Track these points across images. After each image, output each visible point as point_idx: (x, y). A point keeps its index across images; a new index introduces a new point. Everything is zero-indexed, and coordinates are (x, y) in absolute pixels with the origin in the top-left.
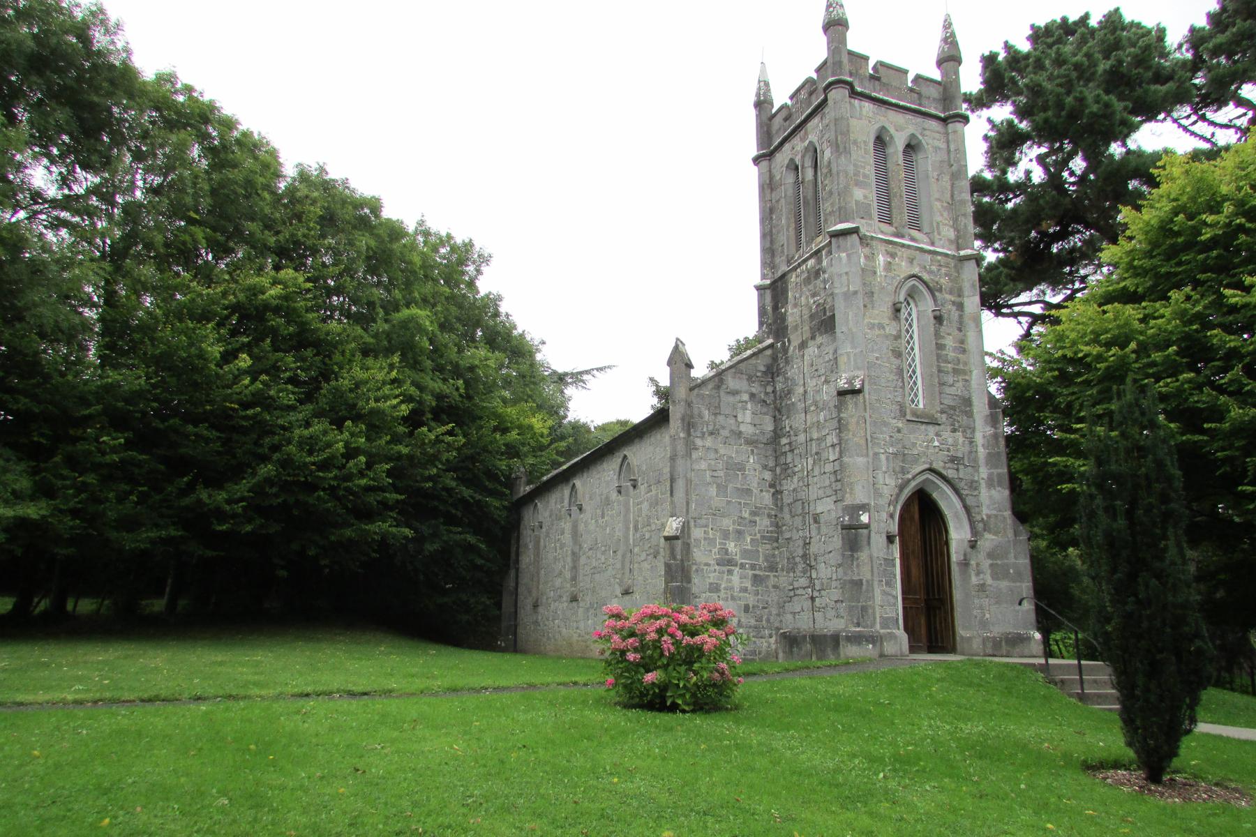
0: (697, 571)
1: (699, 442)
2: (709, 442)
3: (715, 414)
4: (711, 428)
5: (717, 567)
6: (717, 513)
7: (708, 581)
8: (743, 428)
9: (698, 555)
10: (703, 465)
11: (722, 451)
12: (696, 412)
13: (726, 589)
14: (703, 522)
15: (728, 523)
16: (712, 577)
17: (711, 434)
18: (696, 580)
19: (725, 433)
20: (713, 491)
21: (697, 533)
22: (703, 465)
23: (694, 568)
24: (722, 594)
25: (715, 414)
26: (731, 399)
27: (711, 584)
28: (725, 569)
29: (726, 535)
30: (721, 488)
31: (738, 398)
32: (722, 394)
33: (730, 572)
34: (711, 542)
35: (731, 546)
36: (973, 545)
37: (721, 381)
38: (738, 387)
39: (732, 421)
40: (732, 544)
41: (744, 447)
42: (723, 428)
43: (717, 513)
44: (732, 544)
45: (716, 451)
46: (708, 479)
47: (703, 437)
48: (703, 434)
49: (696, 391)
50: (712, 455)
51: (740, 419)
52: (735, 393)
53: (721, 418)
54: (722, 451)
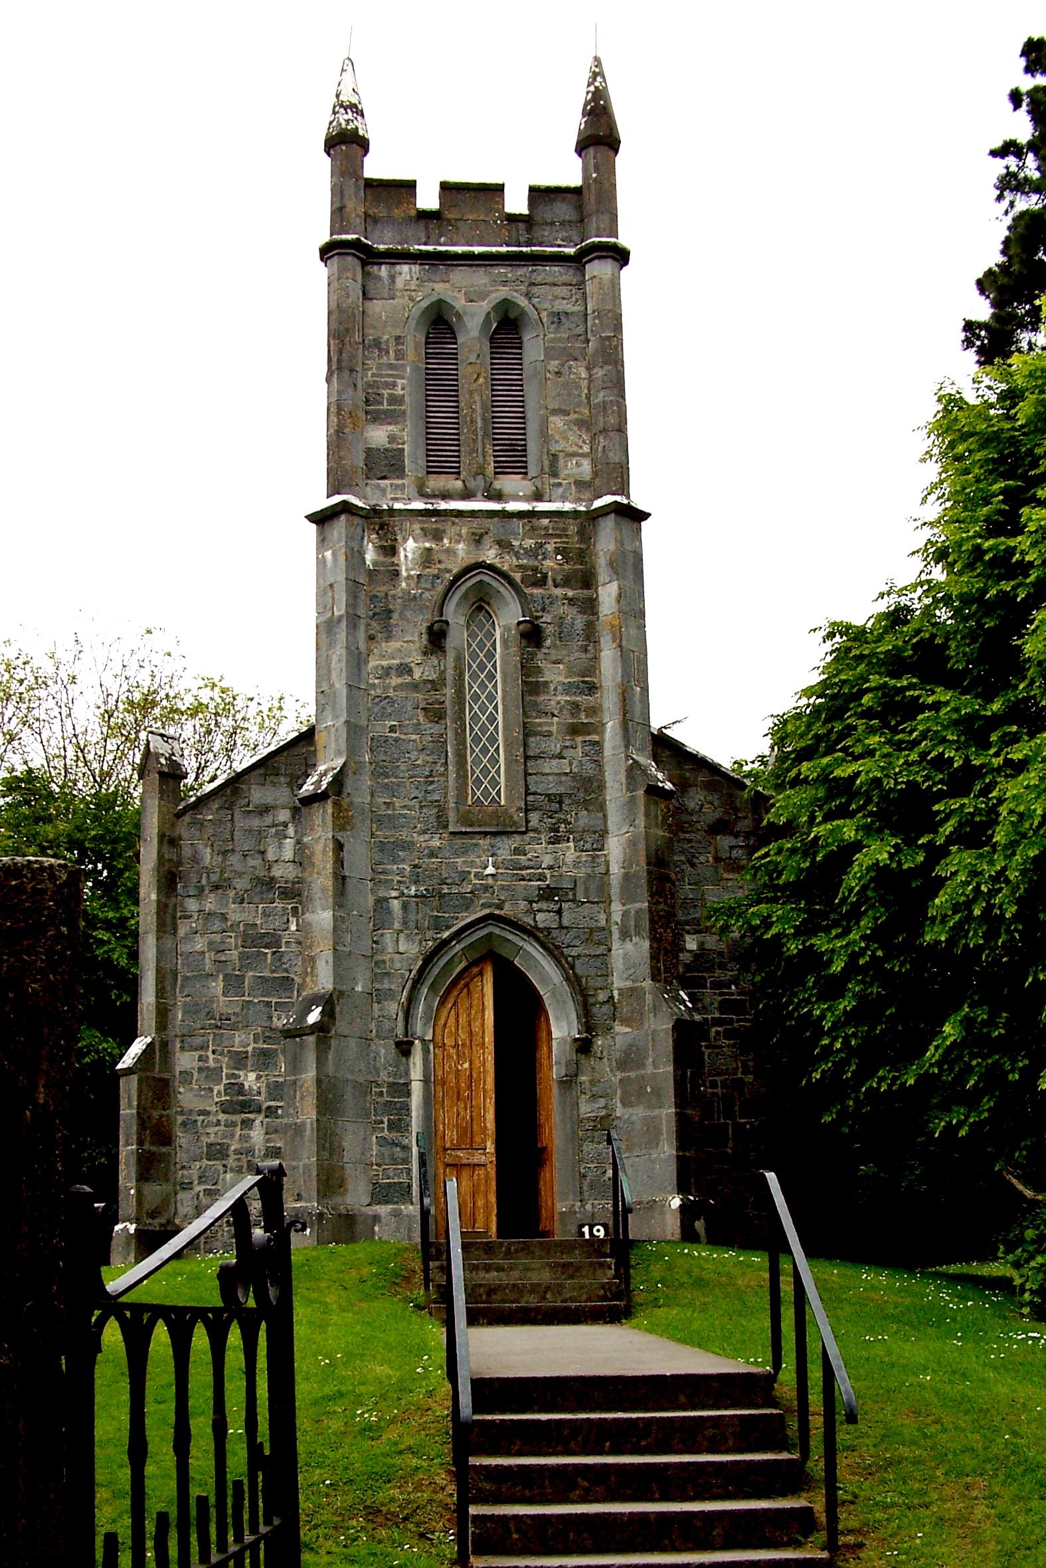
0: (184, 1124)
1: (192, 905)
2: (211, 903)
3: (224, 853)
4: (215, 878)
5: (222, 1117)
6: (224, 1023)
7: (205, 1140)
8: (277, 872)
9: (187, 1097)
10: (200, 944)
11: (234, 917)
12: (187, 852)
13: (237, 1152)
14: (198, 1041)
15: (243, 1041)
16: (213, 1135)
18: (182, 1138)
19: (241, 884)
20: (217, 986)
21: (185, 1061)
22: (200, 944)
23: (180, 1119)
24: (231, 1161)
25: (224, 853)
26: (255, 822)
27: (210, 1145)
28: (237, 1118)
29: (240, 1060)
30: (234, 983)
31: (268, 820)
32: (238, 815)
33: (247, 1124)
34: (213, 1074)
35: (250, 1079)
36: (584, 1046)
38: (269, 800)
39: (255, 862)
40: (252, 1076)
41: (279, 905)
42: (240, 875)
43: (224, 1023)
44: (252, 1076)
45: (224, 918)
46: (208, 966)
47: (200, 894)
48: (201, 890)
49: (187, 819)
50: (217, 925)
51: (271, 856)
52: (265, 810)
53: (234, 860)
54: (234, 917)
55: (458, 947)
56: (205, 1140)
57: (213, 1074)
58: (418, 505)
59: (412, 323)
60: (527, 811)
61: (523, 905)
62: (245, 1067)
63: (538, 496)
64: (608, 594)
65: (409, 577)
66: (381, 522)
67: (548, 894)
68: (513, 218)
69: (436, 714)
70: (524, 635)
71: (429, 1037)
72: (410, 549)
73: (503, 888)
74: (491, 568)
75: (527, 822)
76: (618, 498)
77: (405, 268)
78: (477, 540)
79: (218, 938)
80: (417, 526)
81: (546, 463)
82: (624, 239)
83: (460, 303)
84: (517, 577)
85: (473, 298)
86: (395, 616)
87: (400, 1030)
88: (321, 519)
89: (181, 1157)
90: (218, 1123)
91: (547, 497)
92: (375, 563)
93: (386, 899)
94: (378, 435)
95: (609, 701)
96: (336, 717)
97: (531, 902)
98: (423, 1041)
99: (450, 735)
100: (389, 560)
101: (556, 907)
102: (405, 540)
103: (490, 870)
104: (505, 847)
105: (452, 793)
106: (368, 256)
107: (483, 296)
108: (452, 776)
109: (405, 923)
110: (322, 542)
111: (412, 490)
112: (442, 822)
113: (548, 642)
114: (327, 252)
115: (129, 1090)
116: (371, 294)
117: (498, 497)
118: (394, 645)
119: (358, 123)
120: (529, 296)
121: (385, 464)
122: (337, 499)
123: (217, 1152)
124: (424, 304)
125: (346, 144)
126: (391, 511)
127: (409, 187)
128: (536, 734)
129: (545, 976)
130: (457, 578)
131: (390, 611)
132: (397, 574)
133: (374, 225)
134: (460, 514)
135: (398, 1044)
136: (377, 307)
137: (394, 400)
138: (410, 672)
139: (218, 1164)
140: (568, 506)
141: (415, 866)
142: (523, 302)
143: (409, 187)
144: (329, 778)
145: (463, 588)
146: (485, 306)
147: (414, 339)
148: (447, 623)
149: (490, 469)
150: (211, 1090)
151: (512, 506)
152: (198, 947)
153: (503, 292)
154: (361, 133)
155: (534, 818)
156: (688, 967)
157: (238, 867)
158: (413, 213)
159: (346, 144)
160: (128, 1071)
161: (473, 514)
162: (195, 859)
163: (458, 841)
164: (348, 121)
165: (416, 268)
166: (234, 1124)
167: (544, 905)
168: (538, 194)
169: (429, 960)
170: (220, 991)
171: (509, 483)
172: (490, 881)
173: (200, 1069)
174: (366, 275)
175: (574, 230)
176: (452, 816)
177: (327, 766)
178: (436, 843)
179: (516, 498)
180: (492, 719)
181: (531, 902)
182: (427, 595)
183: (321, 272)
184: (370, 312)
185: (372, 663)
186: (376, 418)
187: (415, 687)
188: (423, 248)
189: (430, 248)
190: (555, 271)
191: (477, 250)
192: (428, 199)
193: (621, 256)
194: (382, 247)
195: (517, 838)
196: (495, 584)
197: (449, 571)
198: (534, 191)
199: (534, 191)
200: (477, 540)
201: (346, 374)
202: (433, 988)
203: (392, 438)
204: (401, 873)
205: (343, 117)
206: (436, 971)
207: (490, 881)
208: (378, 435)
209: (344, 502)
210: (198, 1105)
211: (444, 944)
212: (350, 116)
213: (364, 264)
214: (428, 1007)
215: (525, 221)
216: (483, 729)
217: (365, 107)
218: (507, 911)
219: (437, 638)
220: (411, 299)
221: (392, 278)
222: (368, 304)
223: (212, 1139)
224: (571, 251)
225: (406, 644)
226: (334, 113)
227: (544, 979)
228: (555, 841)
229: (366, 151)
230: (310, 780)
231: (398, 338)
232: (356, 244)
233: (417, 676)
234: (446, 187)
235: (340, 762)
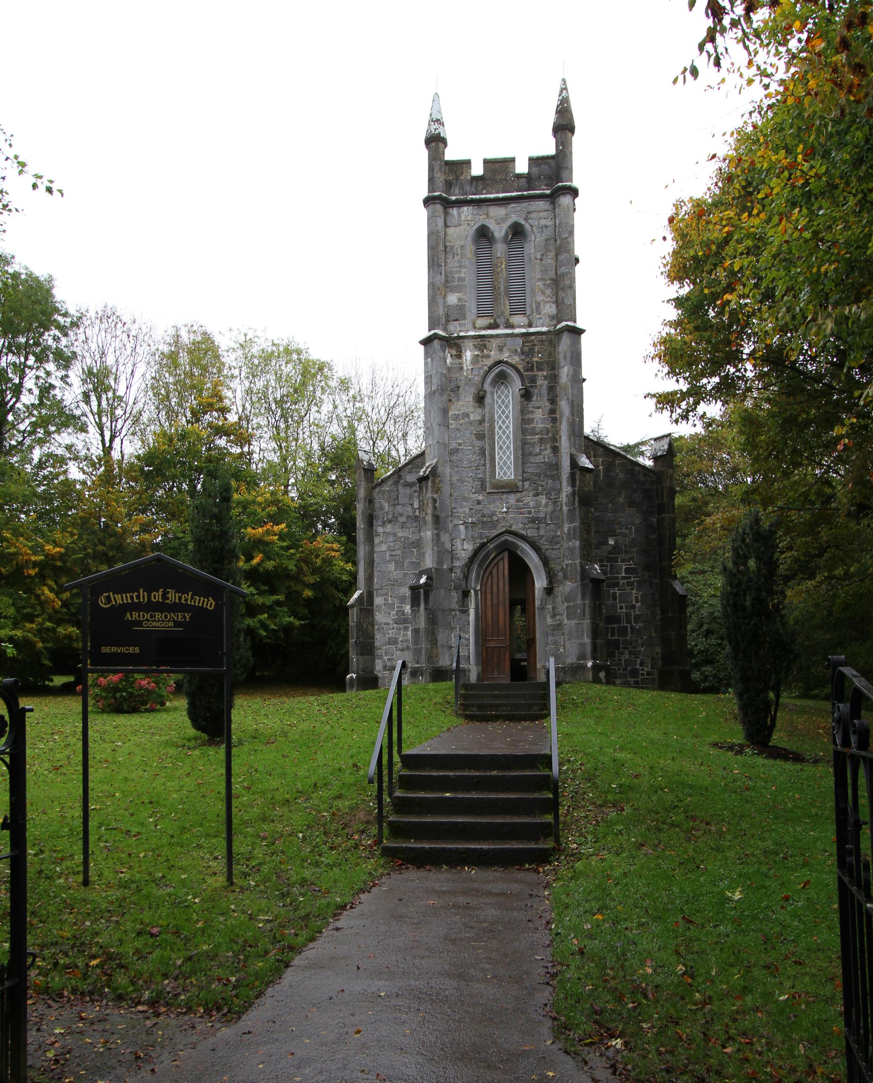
1: (380, 530)
2: (389, 528)
4: (390, 517)
5: (395, 625)
7: (387, 636)
9: (379, 617)
10: (384, 548)
11: (400, 534)
12: (377, 505)
13: (402, 641)
14: (384, 591)
16: (391, 634)
17: (390, 521)
18: (378, 636)
20: (392, 566)
21: (378, 601)
22: (384, 548)
23: (376, 627)
25: (394, 505)
27: (389, 638)
30: (399, 565)
32: (400, 487)
33: (406, 629)
34: (391, 606)
37: (400, 477)
42: (401, 515)
43: (395, 583)
44: (408, 607)
45: (395, 535)
46: (388, 558)
47: (383, 525)
49: (377, 490)
50: (391, 538)
53: (399, 508)
55: (492, 546)
56: (387, 636)
57: (391, 606)
58: (472, 333)
59: (470, 239)
60: (523, 481)
61: (521, 526)
62: (405, 603)
63: (530, 325)
64: (565, 373)
65: (467, 370)
66: (453, 343)
67: (533, 520)
68: (519, 176)
69: (480, 436)
70: (522, 396)
71: (478, 588)
72: (468, 355)
73: (512, 518)
74: (506, 363)
75: (523, 486)
76: (568, 323)
77: (466, 208)
78: (501, 349)
79: (392, 544)
80: (471, 344)
81: (534, 307)
82: (576, 183)
83: (492, 225)
84: (520, 367)
85: (498, 221)
86: (461, 389)
87: (464, 586)
88: (426, 342)
89: (377, 644)
90: (393, 628)
91: (534, 325)
92: (451, 364)
93: (458, 525)
94: (453, 299)
95: (564, 427)
96: (433, 440)
97: (525, 524)
98: (476, 592)
99: (487, 447)
100: (459, 361)
101: (536, 526)
102: (466, 351)
103: (505, 510)
104: (512, 499)
105: (488, 473)
106: (447, 204)
107: (504, 220)
108: (488, 466)
109: (466, 536)
110: (427, 355)
111: (470, 327)
112: (483, 487)
113: (534, 398)
114: (427, 202)
115: (353, 614)
116: (449, 224)
117: (512, 327)
118: (461, 403)
119: (441, 130)
120: (526, 219)
121: (455, 314)
122: (432, 332)
123: (393, 641)
124: (475, 227)
125: (435, 142)
126: (459, 338)
127: (467, 163)
128: (528, 444)
129: (532, 559)
130: (490, 368)
131: (458, 387)
132: (462, 368)
133: (451, 186)
134: (492, 336)
135: (463, 592)
136: (451, 231)
137: (461, 279)
138: (468, 416)
139: (393, 647)
140: (544, 329)
141: (471, 509)
142: (523, 222)
143: (467, 163)
144: (429, 469)
145: (493, 374)
146: (506, 226)
147: (470, 248)
148: (485, 391)
149: (507, 313)
150: (390, 613)
151: (517, 331)
152: (383, 549)
153: (513, 218)
154: (442, 135)
155: (527, 484)
156: (610, 553)
157: (400, 511)
158: (469, 178)
159: (435, 142)
160: (352, 606)
161: (498, 336)
162: (382, 508)
163: (492, 497)
164: (435, 129)
165: (470, 208)
166: (400, 629)
167: (530, 525)
168: (534, 161)
169: (476, 552)
170: (393, 569)
171: (516, 320)
172: (504, 515)
173: (385, 604)
174: (446, 214)
175: (551, 179)
176: (488, 485)
177: (430, 462)
178: (480, 498)
179: (520, 327)
180: (508, 437)
181: (525, 524)
182: (476, 378)
183: (423, 214)
184: (448, 233)
185: (450, 413)
186: (453, 290)
187: (471, 423)
188: (474, 197)
189: (477, 197)
190: (541, 204)
191: (501, 195)
192: (477, 170)
193: (574, 192)
194: (453, 198)
195: (519, 494)
196: (509, 371)
197: (486, 365)
198: (531, 160)
199: (531, 160)
200: (501, 349)
201: (436, 268)
202: (480, 566)
203: (460, 300)
204: (464, 513)
205: (433, 127)
206: (481, 557)
207: (504, 515)
208: (453, 299)
209: (435, 334)
210: (384, 620)
211: (483, 545)
212: (436, 126)
213: (445, 208)
214: (478, 575)
215: (528, 177)
216: (504, 443)
217: (445, 120)
218: (514, 528)
219: (480, 399)
220: (468, 225)
221: (459, 214)
222: (448, 230)
223: (391, 636)
224: (548, 192)
225: (465, 402)
226: (429, 125)
227: (532, 561)
228: (537, 495)
229: (446, 145)
230: (423, 470)
231: (462, 247)
232: (439, 198)
233: (472, 417)
234: (486, 162)
235: (435, 461)
